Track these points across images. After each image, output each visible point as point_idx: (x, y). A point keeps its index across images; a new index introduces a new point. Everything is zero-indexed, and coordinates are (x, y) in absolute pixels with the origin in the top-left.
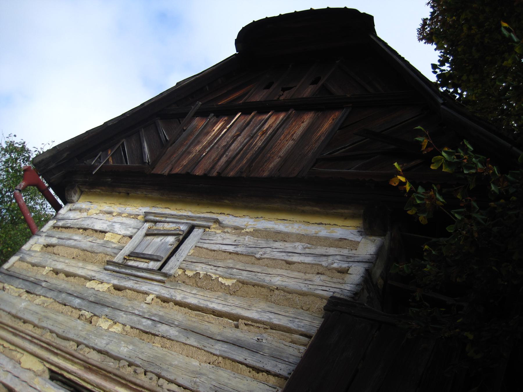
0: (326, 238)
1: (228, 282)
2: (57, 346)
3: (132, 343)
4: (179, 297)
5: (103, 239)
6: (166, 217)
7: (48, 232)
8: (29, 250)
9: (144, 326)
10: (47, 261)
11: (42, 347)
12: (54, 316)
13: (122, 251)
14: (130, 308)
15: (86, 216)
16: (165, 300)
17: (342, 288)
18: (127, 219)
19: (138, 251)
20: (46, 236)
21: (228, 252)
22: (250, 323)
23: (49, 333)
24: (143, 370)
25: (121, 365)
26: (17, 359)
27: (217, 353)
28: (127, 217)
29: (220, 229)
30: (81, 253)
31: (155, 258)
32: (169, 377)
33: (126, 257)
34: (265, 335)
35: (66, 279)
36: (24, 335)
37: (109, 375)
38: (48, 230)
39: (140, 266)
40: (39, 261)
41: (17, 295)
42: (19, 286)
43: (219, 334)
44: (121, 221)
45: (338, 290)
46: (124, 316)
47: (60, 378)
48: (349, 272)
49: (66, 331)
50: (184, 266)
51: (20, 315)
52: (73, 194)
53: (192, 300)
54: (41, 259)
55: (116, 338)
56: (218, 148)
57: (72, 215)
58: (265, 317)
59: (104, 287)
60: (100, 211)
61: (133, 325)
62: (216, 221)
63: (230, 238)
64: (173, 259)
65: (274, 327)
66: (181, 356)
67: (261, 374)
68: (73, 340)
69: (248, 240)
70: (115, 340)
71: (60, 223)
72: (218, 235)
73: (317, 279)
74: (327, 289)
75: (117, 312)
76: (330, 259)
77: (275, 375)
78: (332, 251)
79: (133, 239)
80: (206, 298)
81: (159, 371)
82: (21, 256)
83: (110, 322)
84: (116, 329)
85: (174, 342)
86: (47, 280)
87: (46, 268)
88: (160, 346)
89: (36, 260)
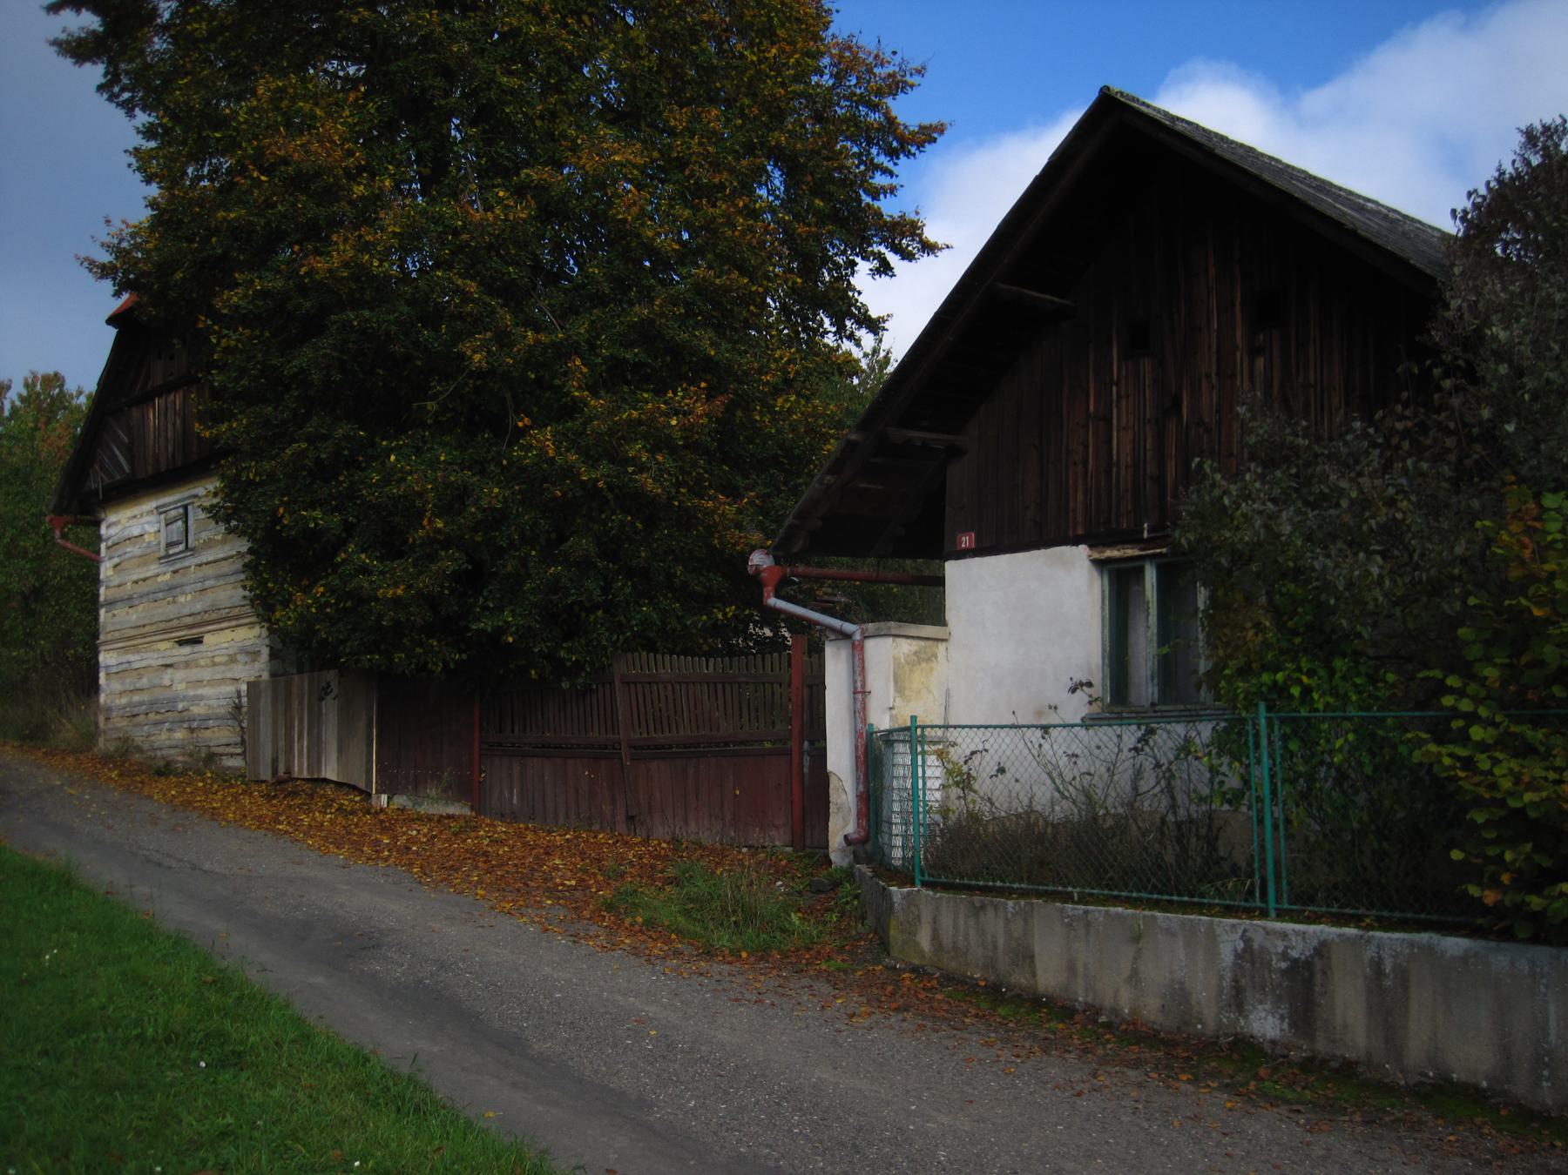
4: (205, 561)
16: (200, 565)
51: (138, 624)
53: (211, 558)
57: (113, 531)
59: (167, 577)
71: (110, 543)
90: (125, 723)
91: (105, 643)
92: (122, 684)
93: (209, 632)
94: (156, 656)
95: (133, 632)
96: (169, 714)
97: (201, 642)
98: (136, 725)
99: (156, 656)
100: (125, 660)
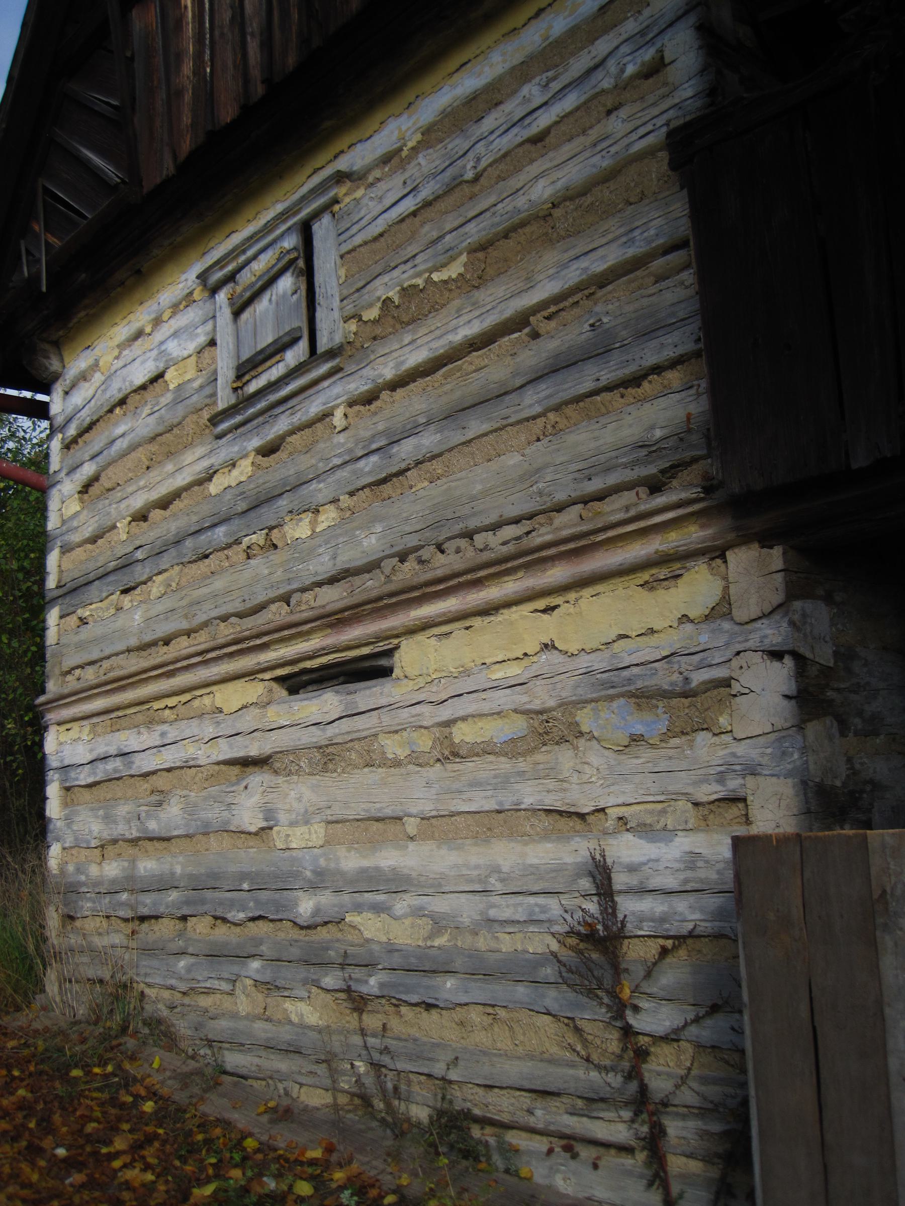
0: (572, 32)
1: (454, 270)
2: (254, 632)
3: (376, 519)
4: (388, 372)
5: (168, 390)
6: (244, 252)
7: (64, 464)
8: (64, 522)
9: (370, 472)
10: (109, 513)
11: (231, 655)
12: (205, 590)
13: (219, 382)
14: (321, 464)
15: (103, 378)
16: (369, 398)
17: (677, 101)
18: (178, 317)
19: (246, 355)
20: (68, 474)
21: (408, 216)
22: (553, 309)
23: (222, 625)
24: (432, 548)
25: (387, 571)
26: (208, 709)
27: (538, 409)
28: (174, 314)
29: (358, 188)
30: (154, 447)
31: (286, 339)
32: (487, 522)
33: (235, 385)
34: (599, 308)
35: (167, 513)
36: (185, 663)
37: (381, 604)
38: (62, 462)
39: (273, 379)
40: (96, 525)
41: (112, 611)
42: (104, 595)
43: (514, 374)
44: (172, 331)
45: (672, 113)
46: (321, 485)
47: (305, 678)
48: (667, 61)
49: (247, 598)
50: (350, 309)
51: (148, 638)
52: (45, 361)
53: (415, 358)
54: (97, 518)
55: (340, 535)
56: (222, 35)
57: (77, 398)
58: (573, 275)
59: (245, 469)
60: (118, 346)
61: (351, 488)
62: (340, 177)
63: (392, 187)
64: (320, 314)
65: (603, 281)
66: (478, 470)
67: (645, 384)
68: (272, 601)
69: (426, 162)
70: (341, 540)
71: (72, 431)
72: (365, 201)
73: (616, 125)
74: (649, 127)
75: (305, 490)
76: (612, 66)
77: (674, 364)
78: (602, 47)
79: (218, 342)
80: (438, 333)
81: (461, 525)
82: (59, 544)
83: (307, 518)
84: (327, 519)
85: (447, 455)
86: (138, 543)
87: (118, 525)
88: (426, 483)
89: (90, 529)
90: (117, 939)
91: (60, 700)
92: (108, 819)
93: (411, 631)
94: (210, 730)
95: (134, 663)
96: (262, 928)
97: (386, 672)
98: (148, 950)
99: (210, 730)
100: (113, 750)
